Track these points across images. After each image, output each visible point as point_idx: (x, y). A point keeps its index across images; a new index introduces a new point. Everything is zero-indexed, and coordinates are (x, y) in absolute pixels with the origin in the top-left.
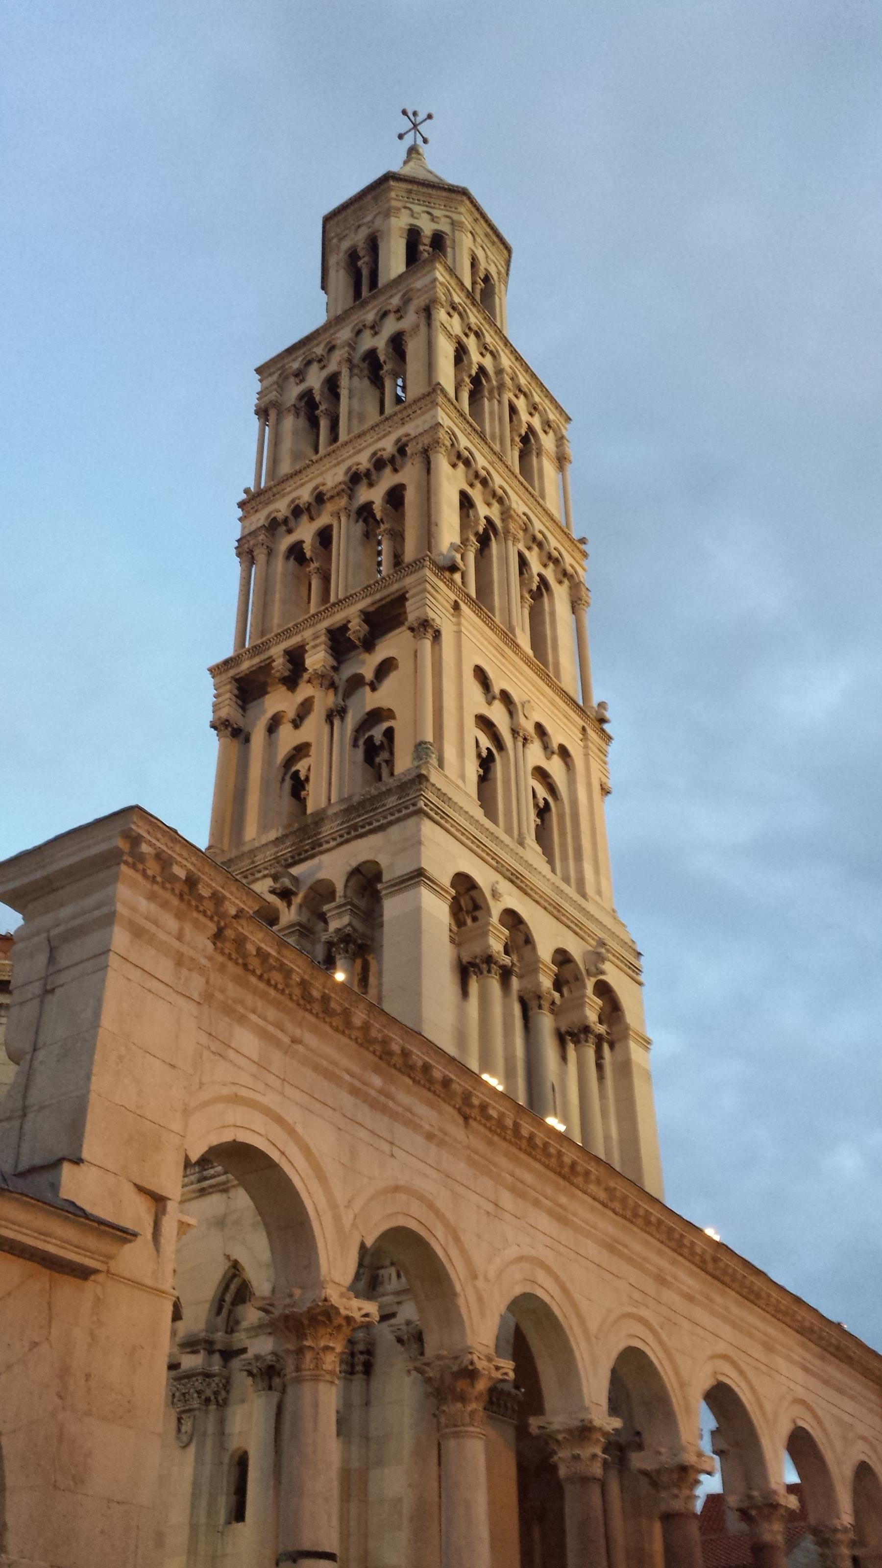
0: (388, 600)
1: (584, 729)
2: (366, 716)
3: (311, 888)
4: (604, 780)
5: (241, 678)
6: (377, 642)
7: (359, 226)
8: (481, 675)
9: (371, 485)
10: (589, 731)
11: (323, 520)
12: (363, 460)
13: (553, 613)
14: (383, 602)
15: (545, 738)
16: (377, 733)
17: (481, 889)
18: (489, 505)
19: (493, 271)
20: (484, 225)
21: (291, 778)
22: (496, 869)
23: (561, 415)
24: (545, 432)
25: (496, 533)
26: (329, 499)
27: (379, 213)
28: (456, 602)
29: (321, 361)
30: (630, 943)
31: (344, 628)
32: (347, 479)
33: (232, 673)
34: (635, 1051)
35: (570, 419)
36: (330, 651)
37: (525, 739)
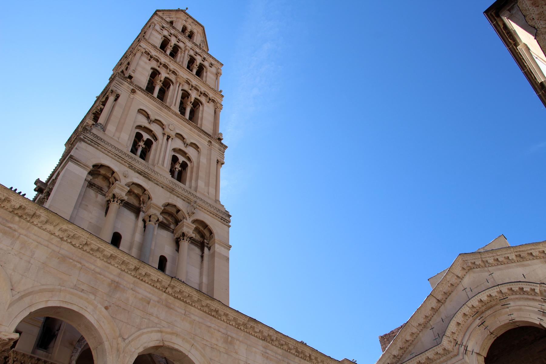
1: (210, 142)
4: (219, 159)
8: (141, 111)
10: (213, 142)
13: (203, 111)
15: (185, 140)
17: (116, 172)
18: (168, 74)
19: (195, 31)
20: (191, 19)
22: (129, 167)
23: (218, 63)
24: (211, 67)
25: (173, 83)
28: (133, 89)
30: (225, 211)
34: (218, 248)
35: (223, 65)
36: (92, 119)
37: (168, 137)
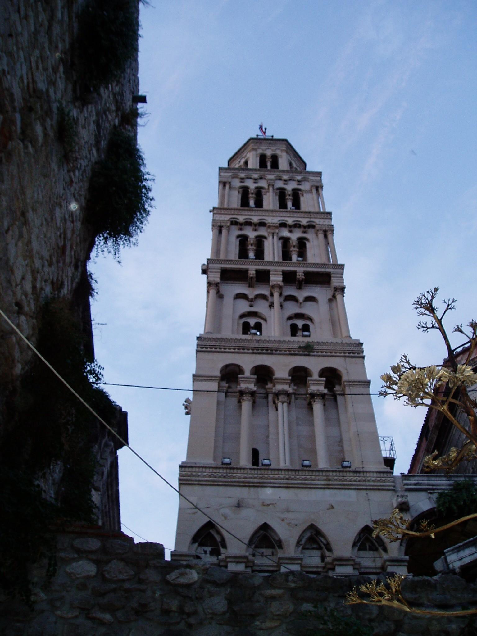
29: (256, 181)
31: (294, 273)
32: (279, 223)
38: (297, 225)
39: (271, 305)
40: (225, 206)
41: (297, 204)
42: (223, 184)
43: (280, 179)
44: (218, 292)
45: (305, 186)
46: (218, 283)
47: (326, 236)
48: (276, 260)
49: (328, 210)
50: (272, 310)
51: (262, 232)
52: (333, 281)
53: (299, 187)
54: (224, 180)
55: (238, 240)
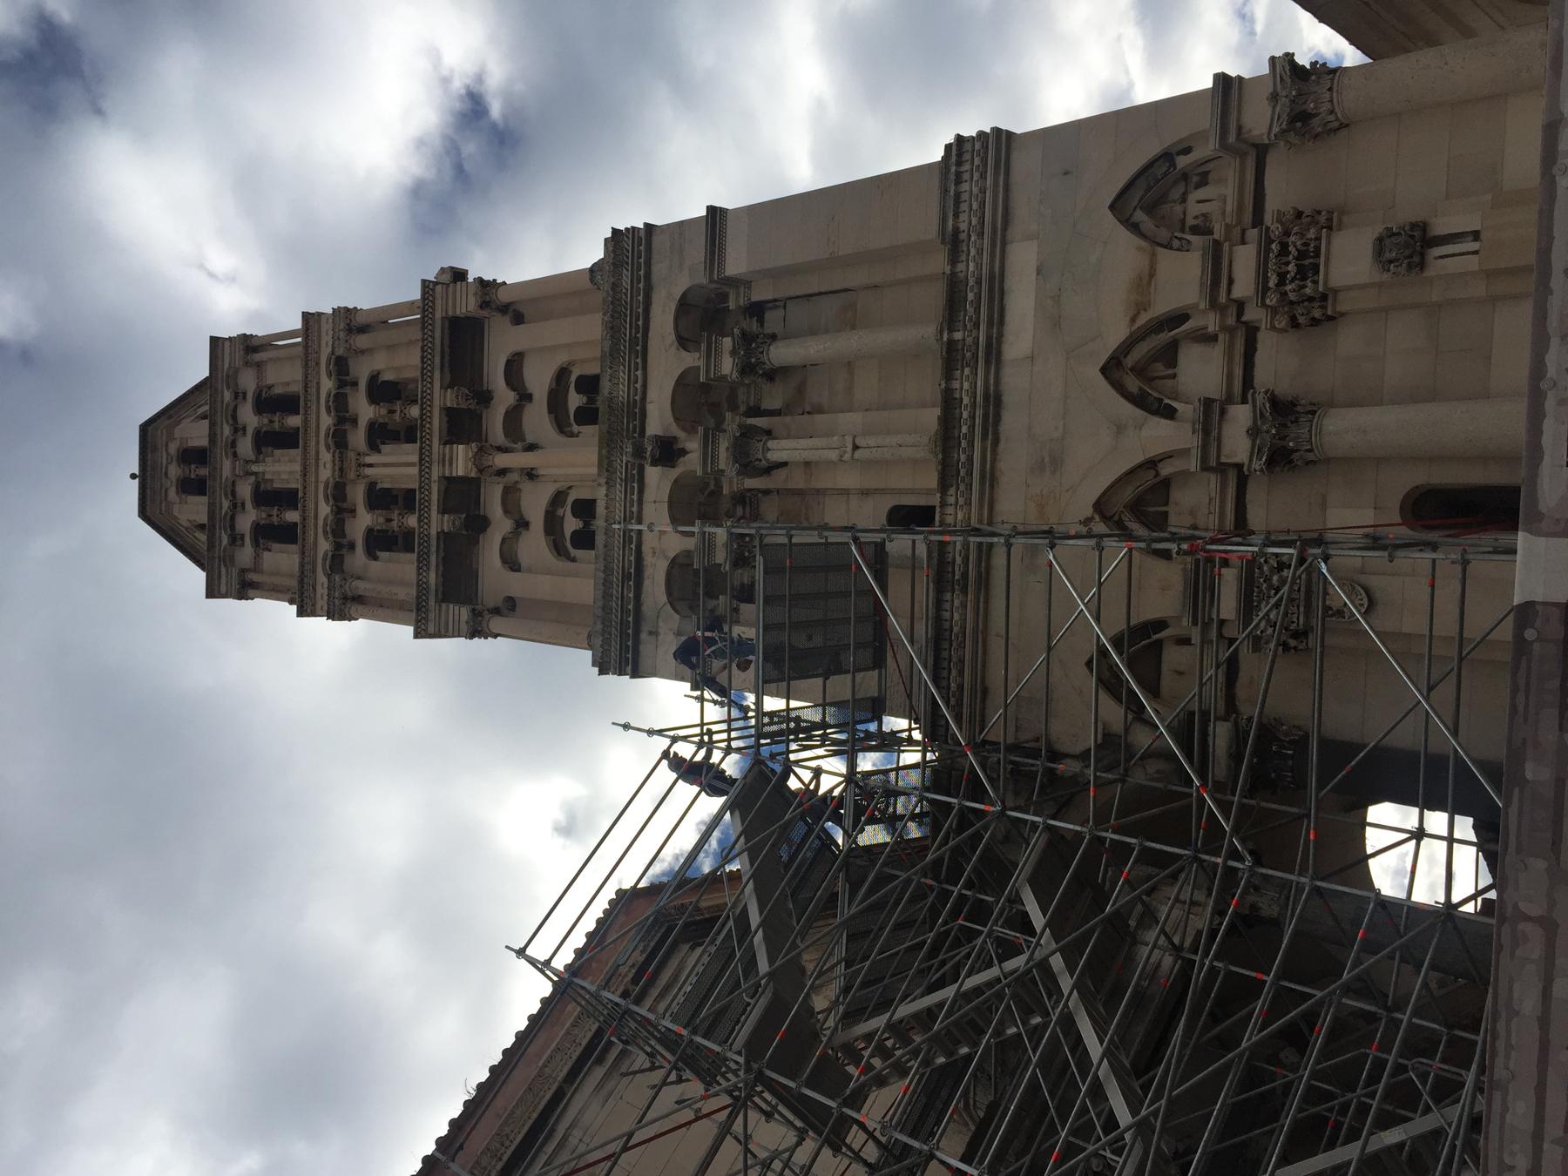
0: (447, 350)
2: (553, 416)
3: (677, 419)
5: (443, 593)
6: (485, 388)
7: (166, 474)
9: (354, 421)
11: (358, 494)
12: (327, 421)
14: (447, 358)
16: (575, 400)
21: (575, 546)
26: (341, 476)
27: (167, 445)
29: (236, 506)
31: (449, 412)
33: (432, 603)
38: (339, 403)
39: (531, 474)
40: (294, 583)
41: (289, 404)
42: (244, 589)
43: (234, 444)
44: (496, 611)
45: (248, 381)
46: (474, 610)
47: (363, 329)
48: (415, 458)
49: (297, 324)
50: (541, 472)
51: (358, 494)
52: (464, 310)
53: (250, 396)
54: (235, 586)
55: (383, 555)
